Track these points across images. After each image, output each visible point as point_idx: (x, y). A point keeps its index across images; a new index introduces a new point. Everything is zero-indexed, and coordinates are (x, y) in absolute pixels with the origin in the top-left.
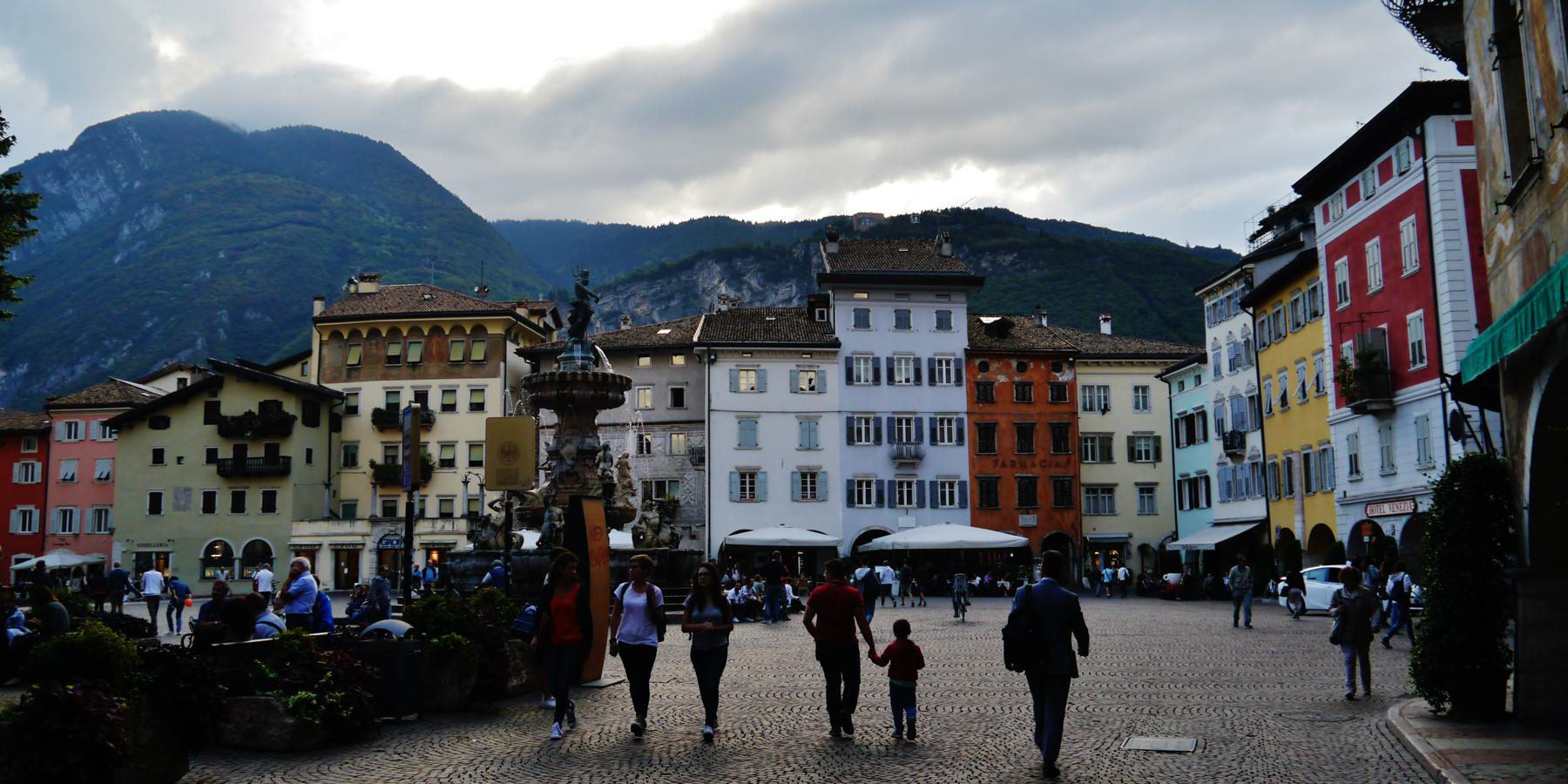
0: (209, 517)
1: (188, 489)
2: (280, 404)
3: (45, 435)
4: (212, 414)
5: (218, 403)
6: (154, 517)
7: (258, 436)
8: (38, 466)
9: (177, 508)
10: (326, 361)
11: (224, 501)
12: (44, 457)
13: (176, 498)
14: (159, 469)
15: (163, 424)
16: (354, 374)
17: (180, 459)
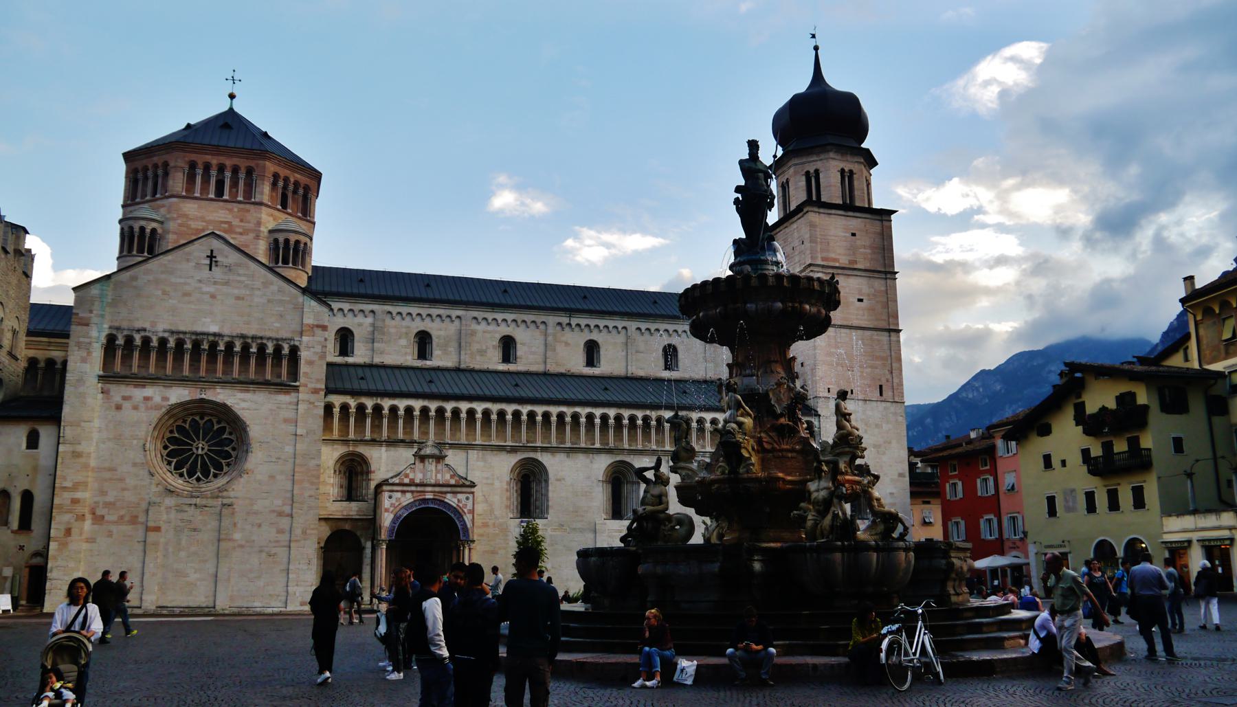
0: (1092, 516)
1: (1073, 491)
2: (1132, 395)
3: (993, 448)
4: (1081, 418)
5: (1083, 403)
6: (1053, 519)
7: (1118, 431)
8: (991, 479)
9: (1069, 509)
10: (1204, 342)
11: (1102, 500)
12: (994, 472)
13: (1066, 501)
14: (1049, 473)
15: (1046, 431)
16: (1232, 348)
17: (1064, 463)
